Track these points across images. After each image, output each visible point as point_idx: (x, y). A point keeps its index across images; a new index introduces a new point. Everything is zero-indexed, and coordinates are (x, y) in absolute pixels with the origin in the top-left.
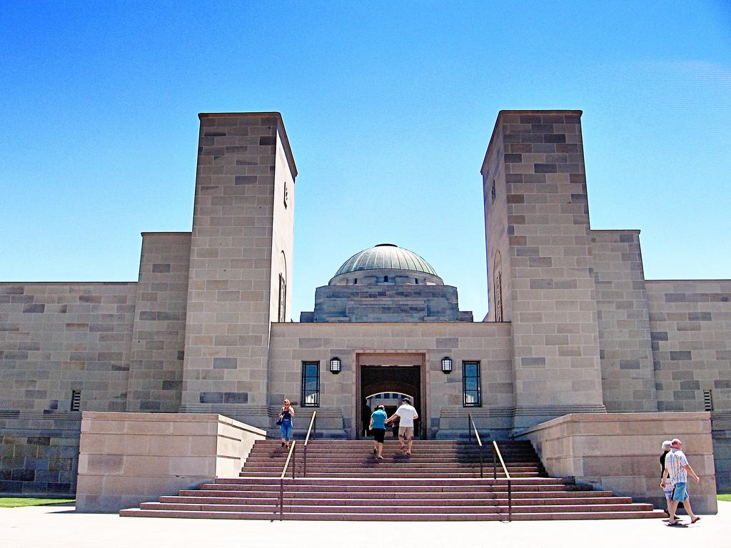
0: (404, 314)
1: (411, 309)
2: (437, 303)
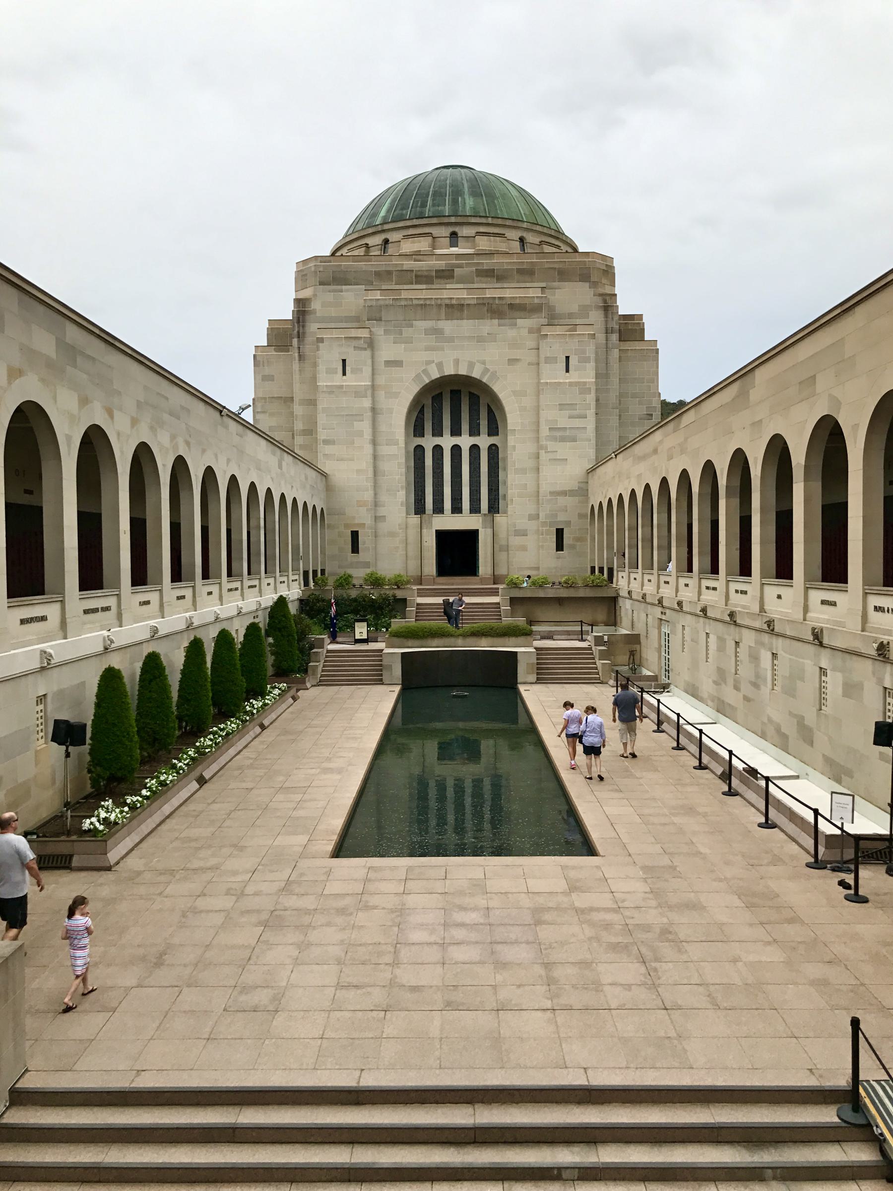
0: (496, 321)
1: (512, 306)
2: (570, 296)
